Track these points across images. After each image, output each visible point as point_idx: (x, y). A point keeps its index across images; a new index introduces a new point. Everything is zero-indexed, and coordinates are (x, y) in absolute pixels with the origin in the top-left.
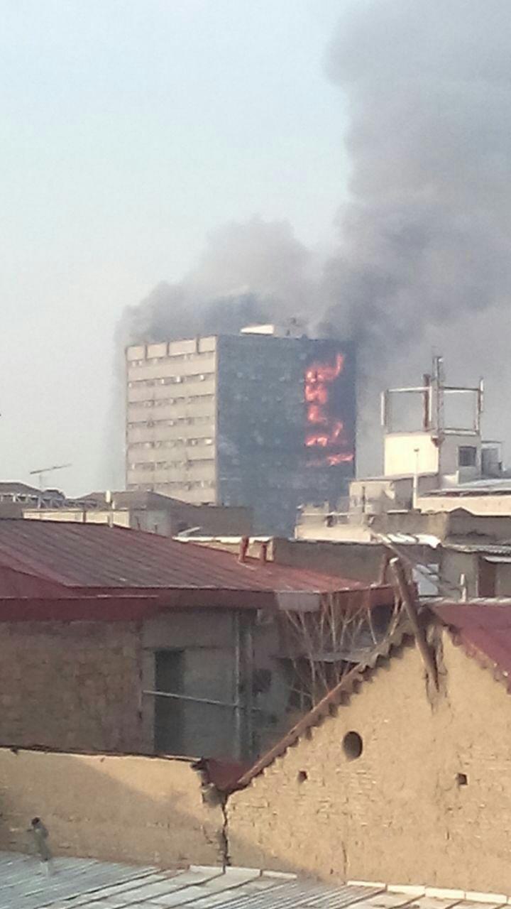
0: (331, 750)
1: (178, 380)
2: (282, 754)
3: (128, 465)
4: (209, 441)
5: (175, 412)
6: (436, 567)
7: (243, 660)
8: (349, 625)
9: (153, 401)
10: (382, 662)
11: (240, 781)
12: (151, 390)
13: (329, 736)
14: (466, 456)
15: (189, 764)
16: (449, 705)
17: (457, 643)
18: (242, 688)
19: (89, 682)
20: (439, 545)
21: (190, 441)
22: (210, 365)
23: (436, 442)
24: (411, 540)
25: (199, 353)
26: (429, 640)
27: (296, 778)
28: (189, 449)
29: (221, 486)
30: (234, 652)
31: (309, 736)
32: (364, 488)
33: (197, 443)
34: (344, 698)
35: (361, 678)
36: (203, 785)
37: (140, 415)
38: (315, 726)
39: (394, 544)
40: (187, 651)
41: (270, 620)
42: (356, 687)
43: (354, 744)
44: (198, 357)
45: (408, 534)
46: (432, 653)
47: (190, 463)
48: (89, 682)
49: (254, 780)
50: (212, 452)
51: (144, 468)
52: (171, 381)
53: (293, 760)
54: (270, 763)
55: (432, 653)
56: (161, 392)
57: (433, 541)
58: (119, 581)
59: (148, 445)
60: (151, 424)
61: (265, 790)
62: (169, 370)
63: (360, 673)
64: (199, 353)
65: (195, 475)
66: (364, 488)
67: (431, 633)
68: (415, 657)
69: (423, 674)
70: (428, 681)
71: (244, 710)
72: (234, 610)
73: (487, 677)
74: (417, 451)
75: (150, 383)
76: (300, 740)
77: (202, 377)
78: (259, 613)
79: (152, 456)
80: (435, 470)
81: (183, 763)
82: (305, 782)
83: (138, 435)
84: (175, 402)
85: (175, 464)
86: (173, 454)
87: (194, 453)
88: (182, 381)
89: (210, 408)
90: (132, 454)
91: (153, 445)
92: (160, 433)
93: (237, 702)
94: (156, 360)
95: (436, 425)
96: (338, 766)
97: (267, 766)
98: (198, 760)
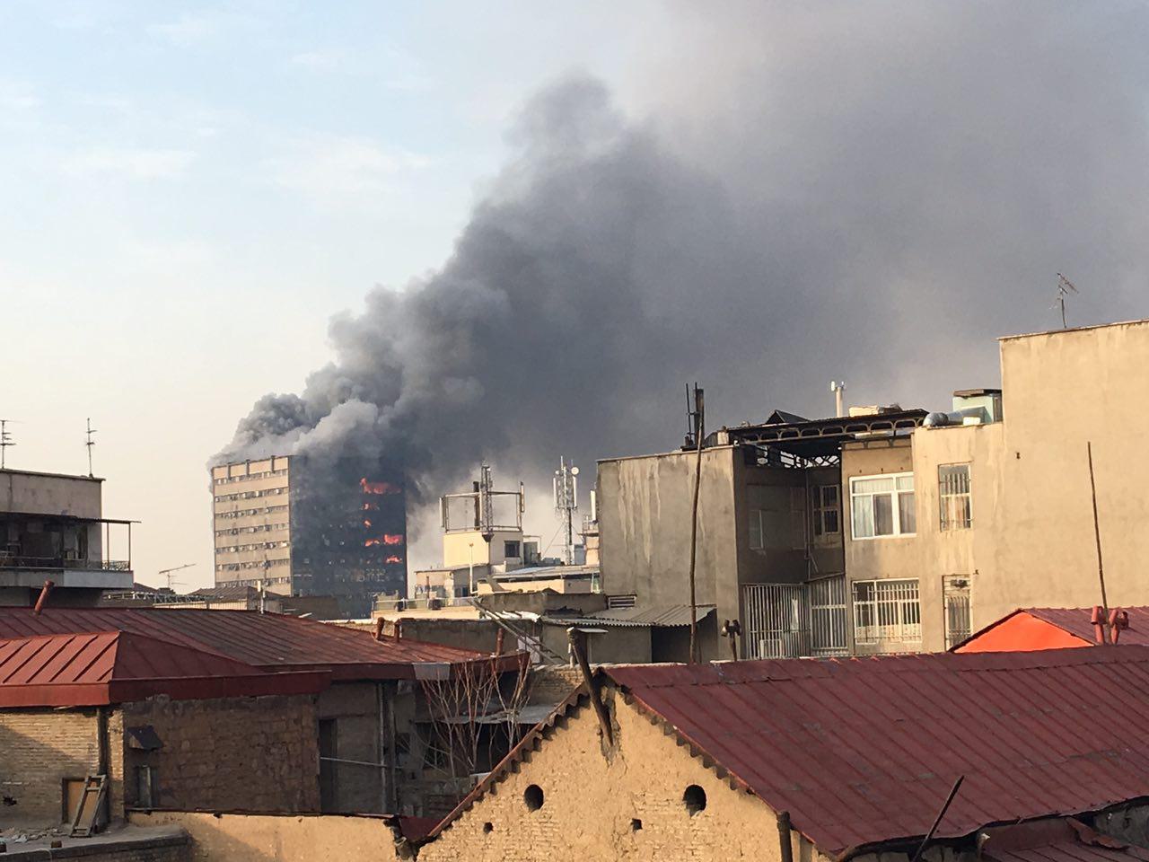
0: (514, 802)
1: (257, 495)
2: (469, 808)
3: (217, 567)
4: (285, 545)
5: (255, 521)
6: (537, 638)
7: (386, 727)
8: (481, 691)
9: (236, 513)
10: (560, 721)
11: (429, 835)
12: (235, 502)
13: (513, 789)
14: (511, 549)
15: (383, 820)
16: (623, 758)
17: (628, 703)
18: (386, 750)
19: (273, 750)
20: (539, 619)
21: (268, 544)
22: (284, 481)
23: (487, 538)
24: (515, 616)
25: (274, 472)
26: (603, 700)
27: (482, 829)
28: (267, 551)
29: (295, 582)
30: (379, 719)
31: (493, 792)
32: (428, 577)
33: (274, 546)
34: (525, 756)
35: (540, 737)
36: (396, 838)
37: (227, 524)
38: (498, 781)
39: (501, 619)
40: (338, 721)
41: (409, 689)
42: (536, 745)
43: (535, 797)
44: (273, 475)
45: (512, 612)
46: (606, 712)
47: (268, 564)
48: (273, 750)
49: (443, 832)
50: (287, 554)
51: (230, 569)
52: (251, 496)
53: (479, 813)
54: (458, 817)
55: (606, 712)
56: (243, 505)
57: (534, 617)
58: (277, 660)
59: (232, 550)
60: (235, 532)
61: (454, 842)
62: (248, 486)
63: (540, 732)
64: (274, 472)
65: (273, 572)
66: (428, 577)
67: (604, 691)
68: (590, 716)
69: (598, 731)
70: (602, 737)
71: (388, 769)
72: (376, 682)
73: (657, 732)
74: (471, 545)
75: (234, 498)
76: (485, 794)
77: (277, 491)
78: (400, 684)
79: (236, 559)
80: (487, 562)
81: (378, 820)
82: (491, 833)
83: (224, 541)
84: (255, 512)
85: (256, 565)
86: (254, 556)
87: (272, 555)
88: (260, 495)
89: (284, 517)
90: (218, 556)
91: (237, 550)
92: (242, 539)
93: (382, 763)
94: (237, 479)
95: (486, 524)
96: (522, 816)
97: (456, 820)
98: (392, 816)
